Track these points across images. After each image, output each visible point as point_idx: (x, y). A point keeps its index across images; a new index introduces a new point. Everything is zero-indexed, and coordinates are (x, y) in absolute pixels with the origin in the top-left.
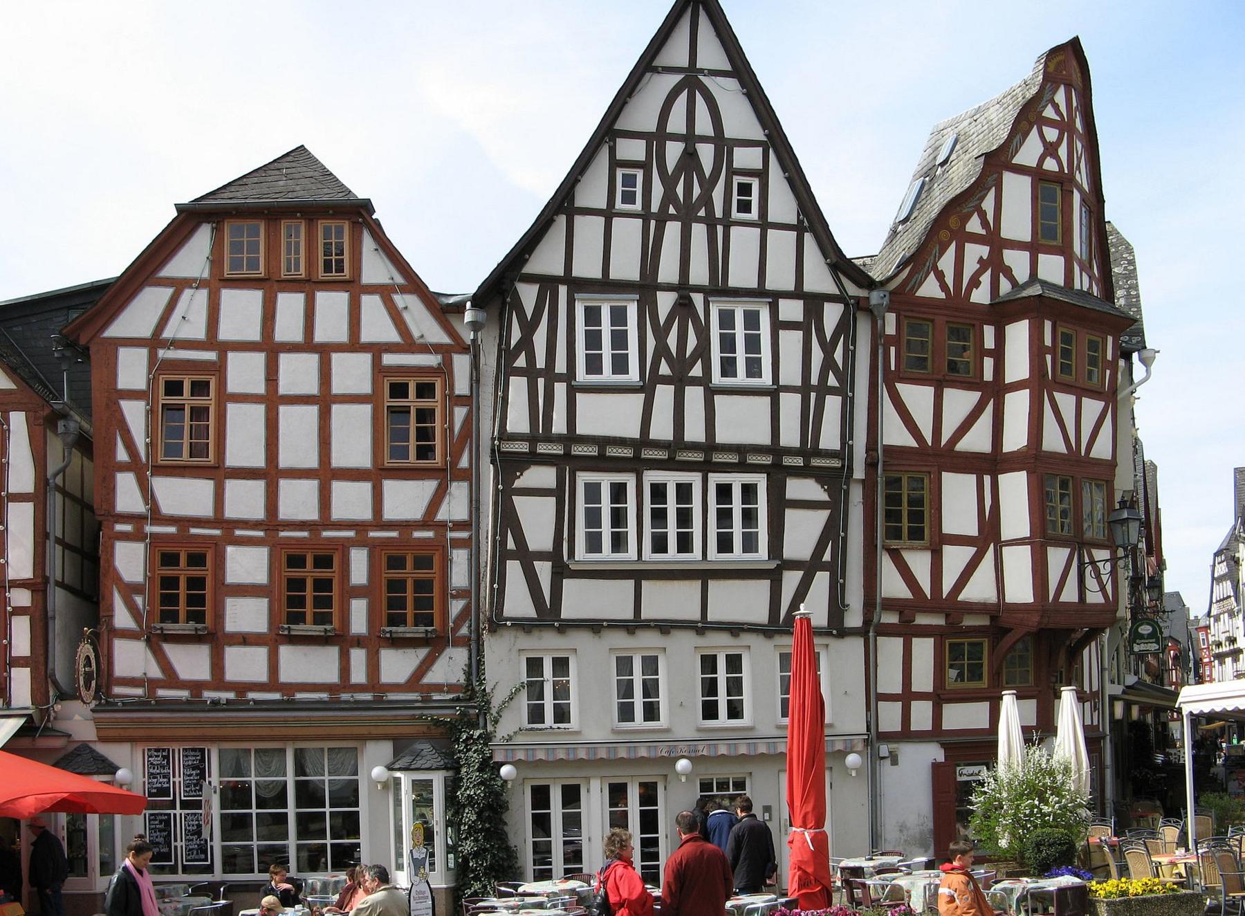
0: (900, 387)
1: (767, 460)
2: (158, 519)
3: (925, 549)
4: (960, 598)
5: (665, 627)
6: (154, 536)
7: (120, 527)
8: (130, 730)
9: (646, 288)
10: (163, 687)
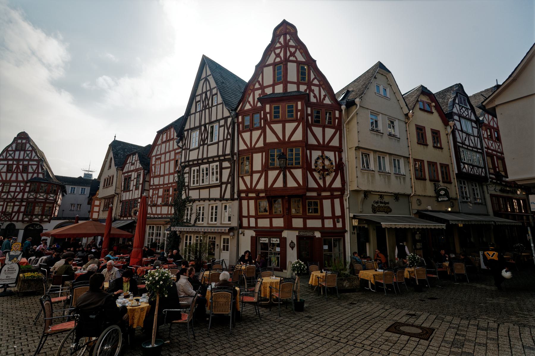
0: (243, 134)
1: (217, 159)
3: (248, 175)
4: (256, 188)
5: (204, 200)
9: (200, 127)
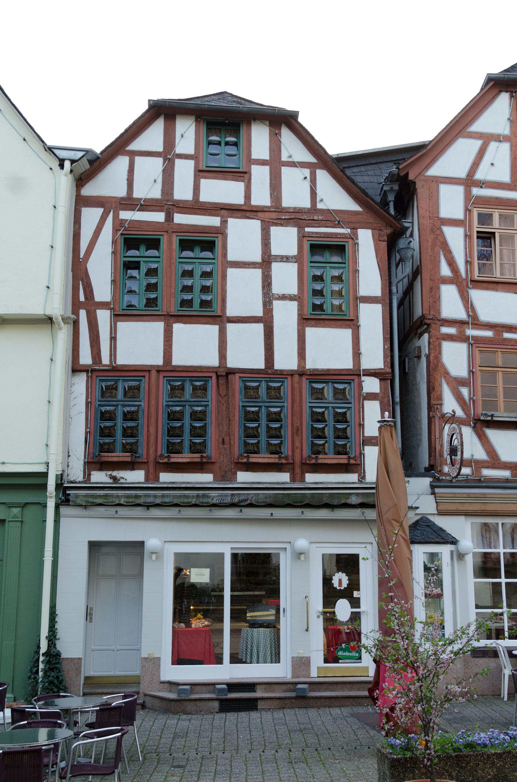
2: (476, 324)
6: (476, 339)
7: (445, 330)
8: (466, 505)
10: (488, 467)
